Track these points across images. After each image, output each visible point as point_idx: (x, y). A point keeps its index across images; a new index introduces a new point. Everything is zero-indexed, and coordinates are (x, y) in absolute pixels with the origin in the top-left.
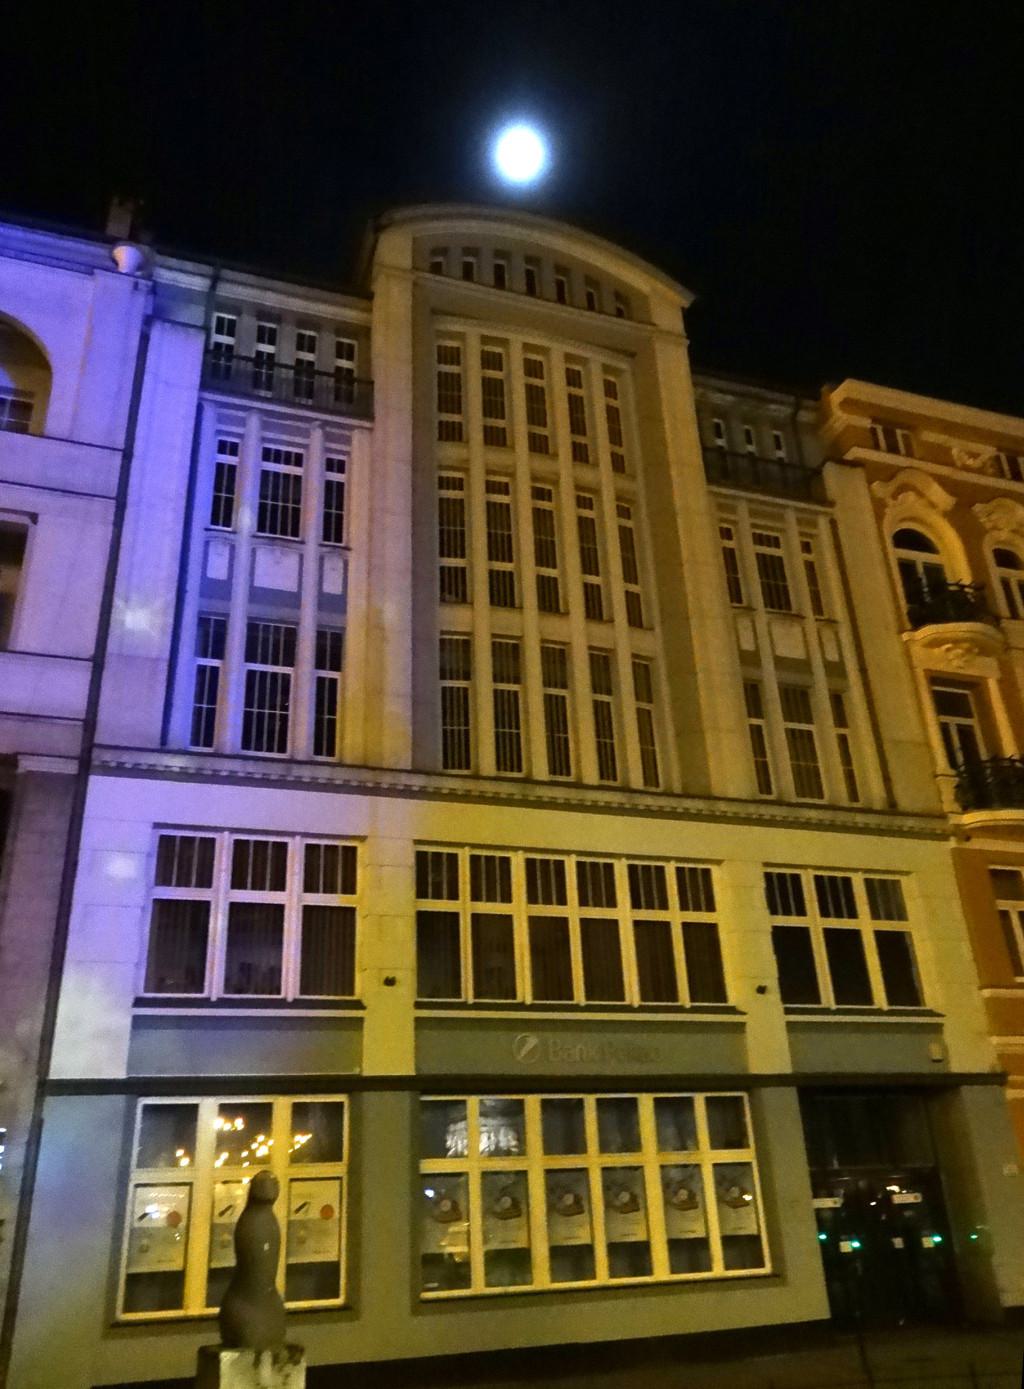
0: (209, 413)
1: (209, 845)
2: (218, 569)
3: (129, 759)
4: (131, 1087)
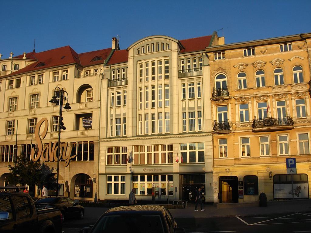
0: (109, 90)
1: (112, 148)
2: (112, 113)
3: (102, 140)
4: (106, 174)
